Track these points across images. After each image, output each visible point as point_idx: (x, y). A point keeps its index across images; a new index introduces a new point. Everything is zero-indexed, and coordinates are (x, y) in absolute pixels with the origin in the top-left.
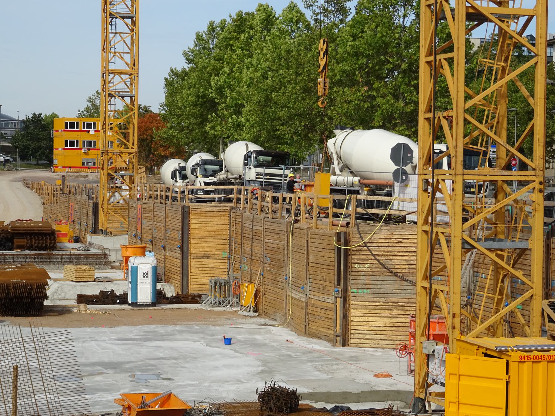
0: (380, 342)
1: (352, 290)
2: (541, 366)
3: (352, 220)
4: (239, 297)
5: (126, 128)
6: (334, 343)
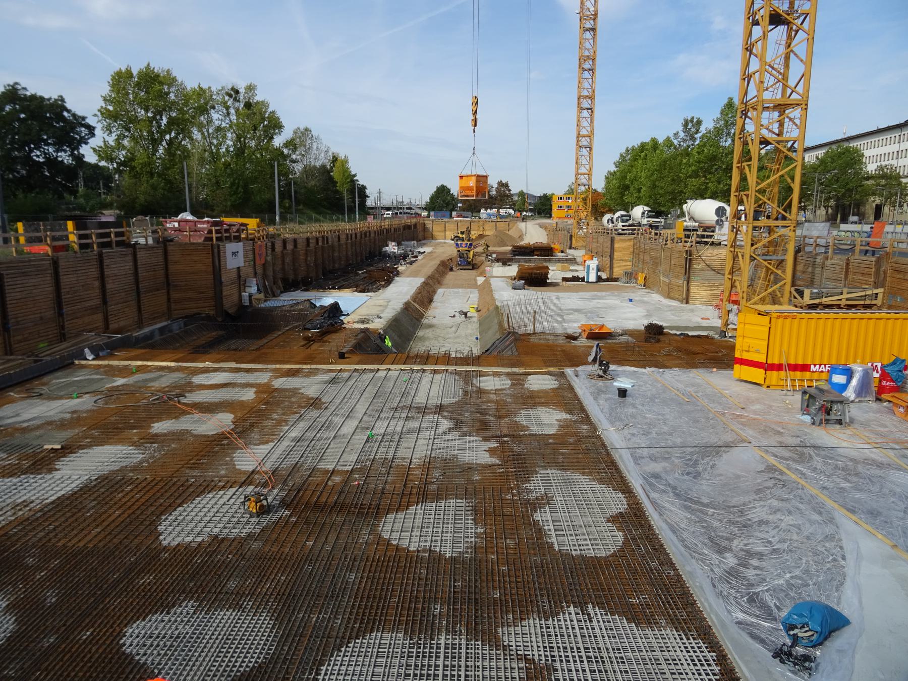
2: (789, 320)
3: (694, 244)
4: (637, 279)
6: (682, 302)
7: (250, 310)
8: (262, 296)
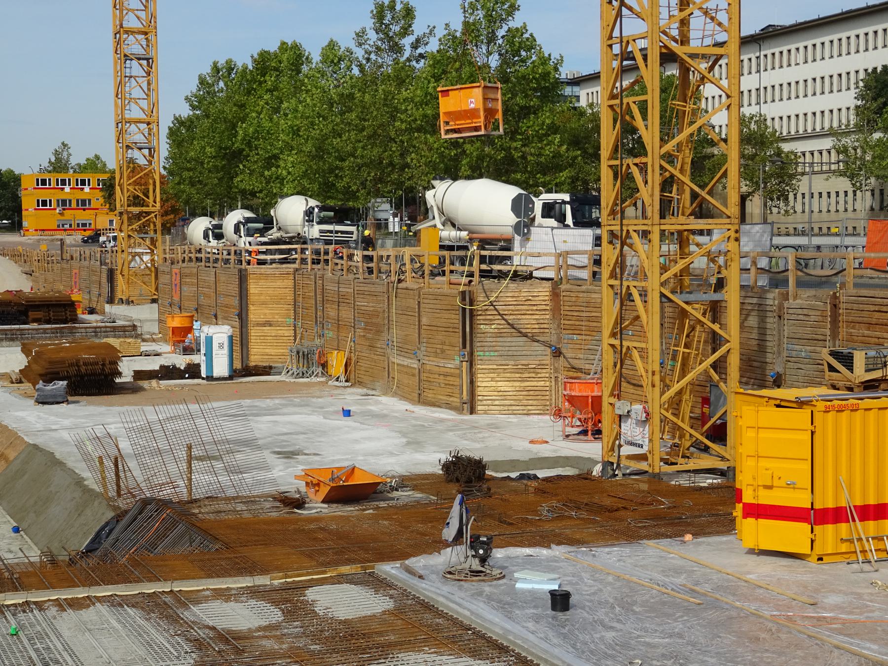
0: (510, 408)
1: (479, 353)
3: (476, 278)
4: (324, 366)
5: (146, 184)
6: (459, 410)
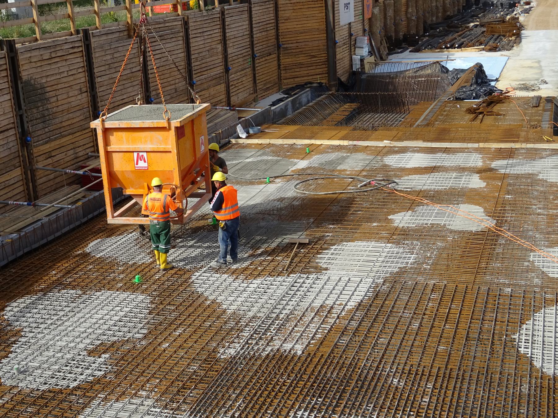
7: (364, 77)
8: (372, 59)
